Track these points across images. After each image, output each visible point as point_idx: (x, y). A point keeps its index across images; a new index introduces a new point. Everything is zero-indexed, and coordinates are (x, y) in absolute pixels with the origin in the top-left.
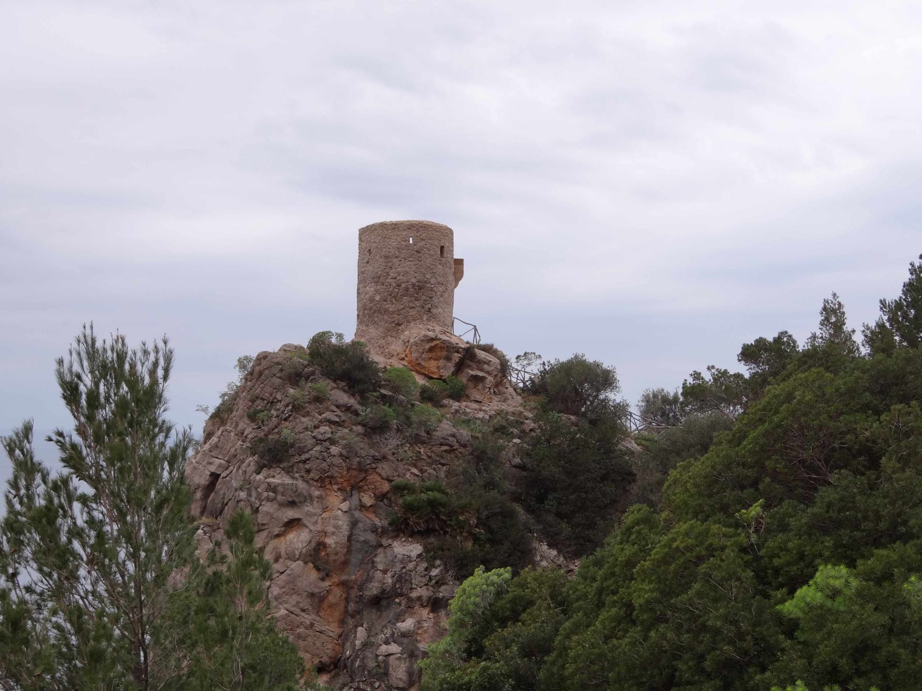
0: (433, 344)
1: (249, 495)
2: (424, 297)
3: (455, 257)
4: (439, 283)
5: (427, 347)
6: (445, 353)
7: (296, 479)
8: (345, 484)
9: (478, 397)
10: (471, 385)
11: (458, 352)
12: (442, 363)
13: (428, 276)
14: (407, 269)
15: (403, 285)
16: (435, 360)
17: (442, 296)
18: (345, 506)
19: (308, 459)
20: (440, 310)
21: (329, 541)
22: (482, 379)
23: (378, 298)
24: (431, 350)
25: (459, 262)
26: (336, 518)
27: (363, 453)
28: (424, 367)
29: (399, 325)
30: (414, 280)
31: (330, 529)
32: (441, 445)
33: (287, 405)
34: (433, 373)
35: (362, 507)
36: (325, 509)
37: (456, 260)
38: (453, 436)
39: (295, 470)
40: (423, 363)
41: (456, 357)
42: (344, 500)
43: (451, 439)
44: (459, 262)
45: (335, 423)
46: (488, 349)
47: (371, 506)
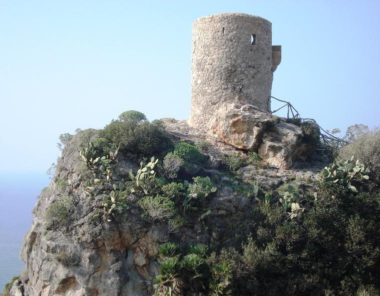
1: (37, 255)
3: (273, 44)
4: (250, 67)
5: (231, 122)
6: (245, 127)
7: (72, 242)
10: (271, 153)
11: (258, 126)
18: (117, 266)
19: (83, 224)
23: (199, 82)
24: (234, 124)
25: (278, 49)
33: (78, 176)
35: (136, 266)
37: (274, 47)
39: (73, 233)
41: (256, 130)
42: (117, 261)
44: (278, 49)
46: (296, 122)
47: (144, 265)
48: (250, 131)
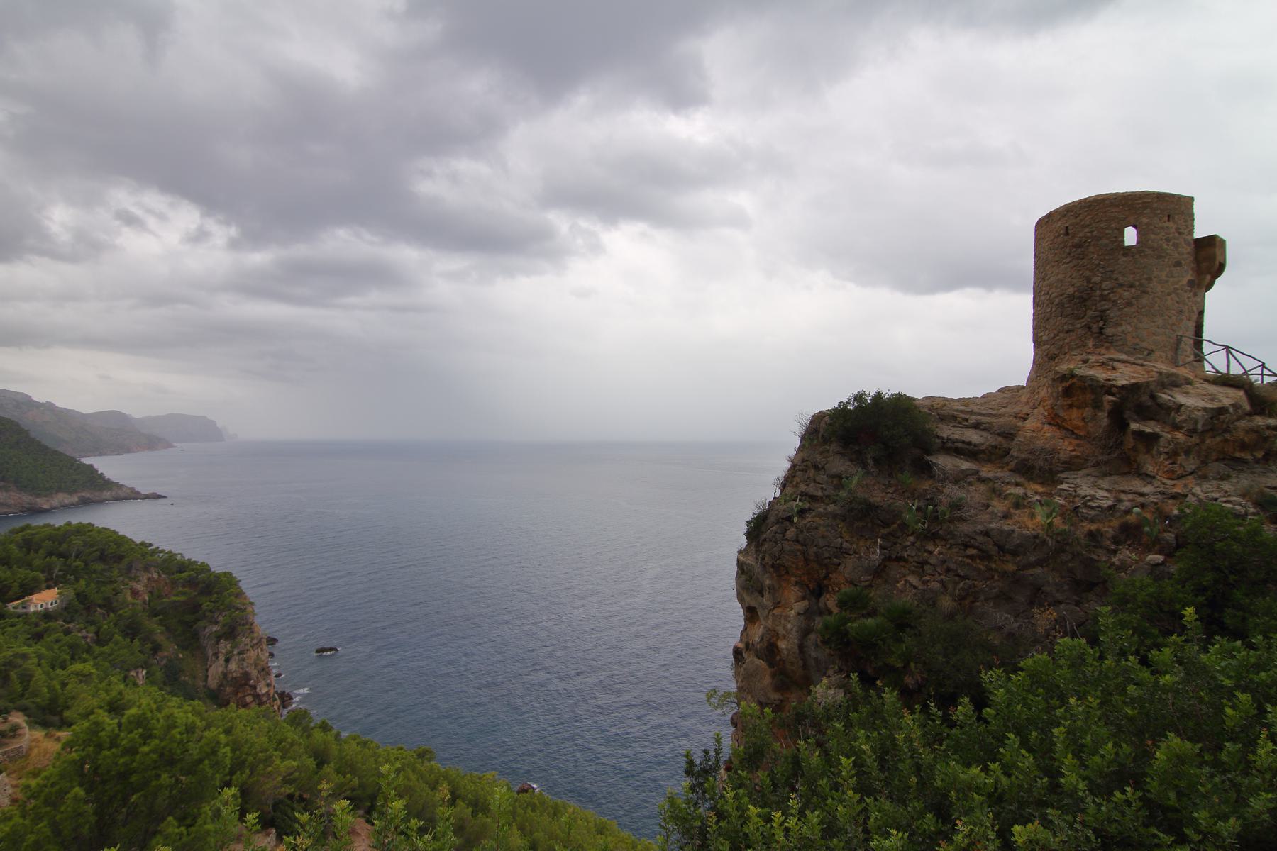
0: (1066, 384)
2: (1090, 313)
4: (1121, 285)
6: (1089, 397)
8: (805, 578)
9: (1150, 468)
12: (1088, 412)
13: (1097, 279)
14: (1060, 277)
15: (1057, 301)
16: (1078, 408)
17: (1129, 304)
20: (1126, 327)
21: (782, 645)
22: (1155, 437)
26: (787, 618)
27: (821, 542)
28: (1064, 420)
29: (1052, 358)
30: (1071, 290)
31: (781, 630)
32: (966, 546)
34: (1078, 428)
36: (777, 604)
38: (986, 533)
40: (1062, 414)
42: (803, 598)
43: (980, 539)
45: (813, 498)
48: (1097, 406)
